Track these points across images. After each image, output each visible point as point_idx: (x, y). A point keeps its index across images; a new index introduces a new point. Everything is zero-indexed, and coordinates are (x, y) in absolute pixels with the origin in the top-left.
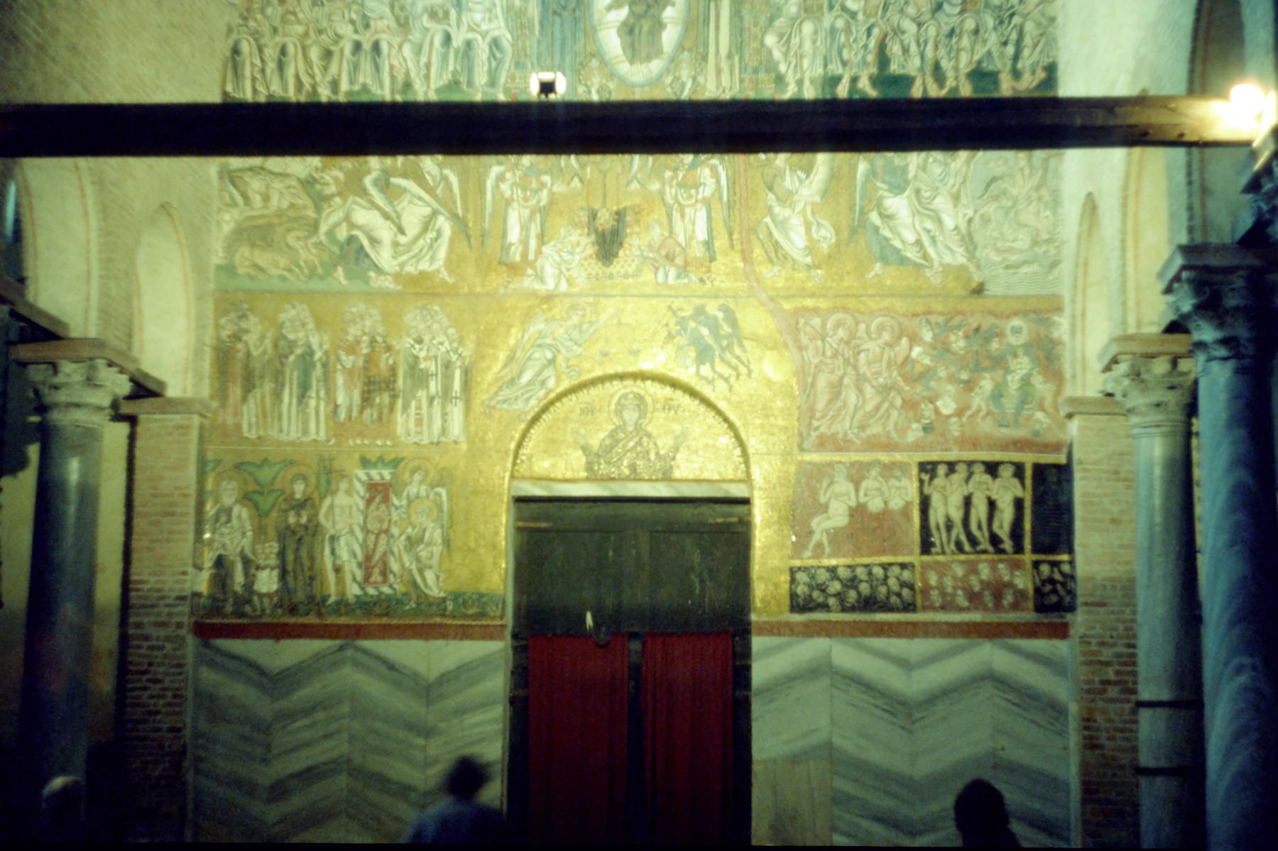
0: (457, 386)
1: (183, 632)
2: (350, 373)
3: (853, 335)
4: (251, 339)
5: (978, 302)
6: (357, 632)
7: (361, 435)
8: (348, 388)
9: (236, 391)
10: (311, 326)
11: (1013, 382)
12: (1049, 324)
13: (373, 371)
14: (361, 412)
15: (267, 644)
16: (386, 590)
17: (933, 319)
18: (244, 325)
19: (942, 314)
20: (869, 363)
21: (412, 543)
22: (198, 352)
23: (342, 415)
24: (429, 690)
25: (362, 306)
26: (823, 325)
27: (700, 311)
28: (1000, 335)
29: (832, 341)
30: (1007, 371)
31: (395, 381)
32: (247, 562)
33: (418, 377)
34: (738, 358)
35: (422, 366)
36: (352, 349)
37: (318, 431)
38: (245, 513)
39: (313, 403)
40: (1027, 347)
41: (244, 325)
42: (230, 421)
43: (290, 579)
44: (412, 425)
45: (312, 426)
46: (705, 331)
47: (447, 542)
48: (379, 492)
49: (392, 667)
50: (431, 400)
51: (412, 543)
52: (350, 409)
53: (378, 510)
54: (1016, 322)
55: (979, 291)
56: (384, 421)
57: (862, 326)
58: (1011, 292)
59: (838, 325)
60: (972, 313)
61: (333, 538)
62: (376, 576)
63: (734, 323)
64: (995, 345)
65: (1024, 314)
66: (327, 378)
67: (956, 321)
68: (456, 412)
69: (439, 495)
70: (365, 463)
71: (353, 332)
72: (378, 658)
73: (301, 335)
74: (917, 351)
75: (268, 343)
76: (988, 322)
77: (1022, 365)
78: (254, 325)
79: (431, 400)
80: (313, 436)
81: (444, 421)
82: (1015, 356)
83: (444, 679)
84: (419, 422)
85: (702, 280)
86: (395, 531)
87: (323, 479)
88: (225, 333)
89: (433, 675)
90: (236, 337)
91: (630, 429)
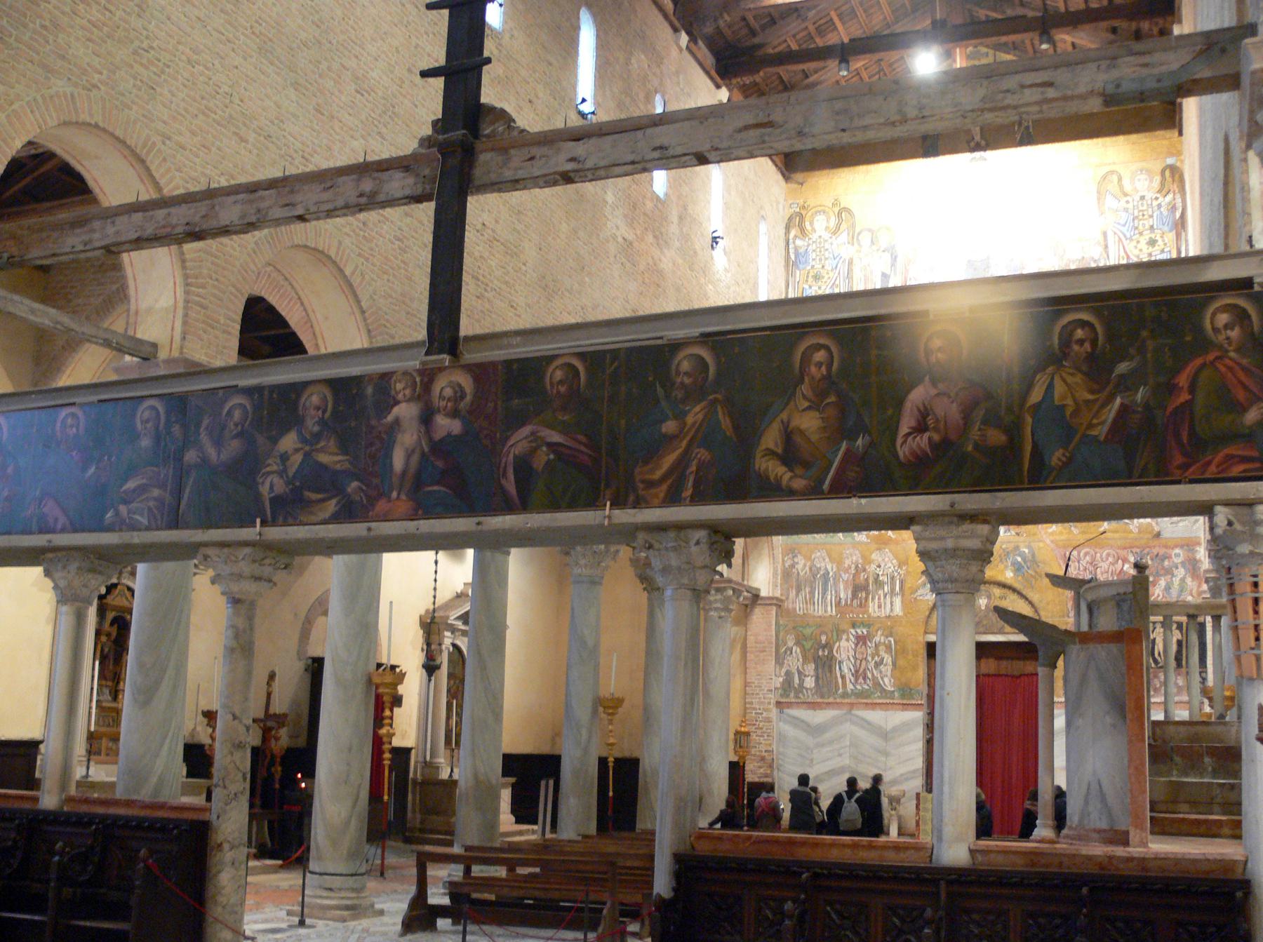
0: (897, 588)
1: (771, 706)
2: (846, 582)
3: (1094, 559)
4: (800, 567)
5: (1156, 542)
6: (852, 705)
7: (852, 612)
8: (845, 589)
9: (793, 593)
10: (827, 560)
11: (1176, 581)
12: (1193, 551)
13: (857, 581)
14: (852, 601)
15: (810, 712)
16: (866, 687)
17: (1134, 550)
18: (796, 560)
19: (1138, 547)
20: (1102, 574)
21: (877, 665)
22: (775, 574)
23: (843, 602)
24: (885, 735)
25: (851, 550)
26: (1079, 555)
27: (1017, 548)
28: (1169, 557)
29: (1084, 563)
30: (1173, 575)
31: (868, 586)
32: (799, 673)
33: (879, 583)
34: (1036, 572)
35: (881, 578)
36: (847, 570)
37: (832, 611)
38: (798, 650)
39: (829, 597)
40: (1183, 563)
41: (796, 560)
42: (790, 606)
43: (820, 682)
44: (876, 609)
45: (829, 608)
46: (1019, 559)
47: (894, 664)
48: (861, 640)
49: (869, 723)
50: (885, 596)
51: (877, 665)
52: (846, 601)
53: (861, 649)
54: (1177, 551)
55: (1158, 535)
56: (863, 605)
57: (1098, 555)
58: (1174, 536)
59: (1086, 554)
60: (1154, 547)
61: (840, 662)
62: (861, 680)
63: (1033, 555)
64: (1166, 563)
65: (1182, 547)
66: (836, 584)
67: (1145, 552)
68: (898, 601)
69: (890, 641)
70: (854, 626)
71: (847, 562)
72: (863, 719)
73: (823, 565)
74: (1126, 566)
75: (807, 568)
76: (1162, 551)
77: (1181, 572)
78: (801, 561)
79: (885, 596)
80: (829, 613)
81: (892, 605)
82: (1177, 568)
83: (895, 729)
84: (880, 607)
85: (1018, 534)
86: (870, 658)
87: (835, 634)
88: (787, 565)
89: (889, 726)
90: (793, 566)
91: (983, 608)
